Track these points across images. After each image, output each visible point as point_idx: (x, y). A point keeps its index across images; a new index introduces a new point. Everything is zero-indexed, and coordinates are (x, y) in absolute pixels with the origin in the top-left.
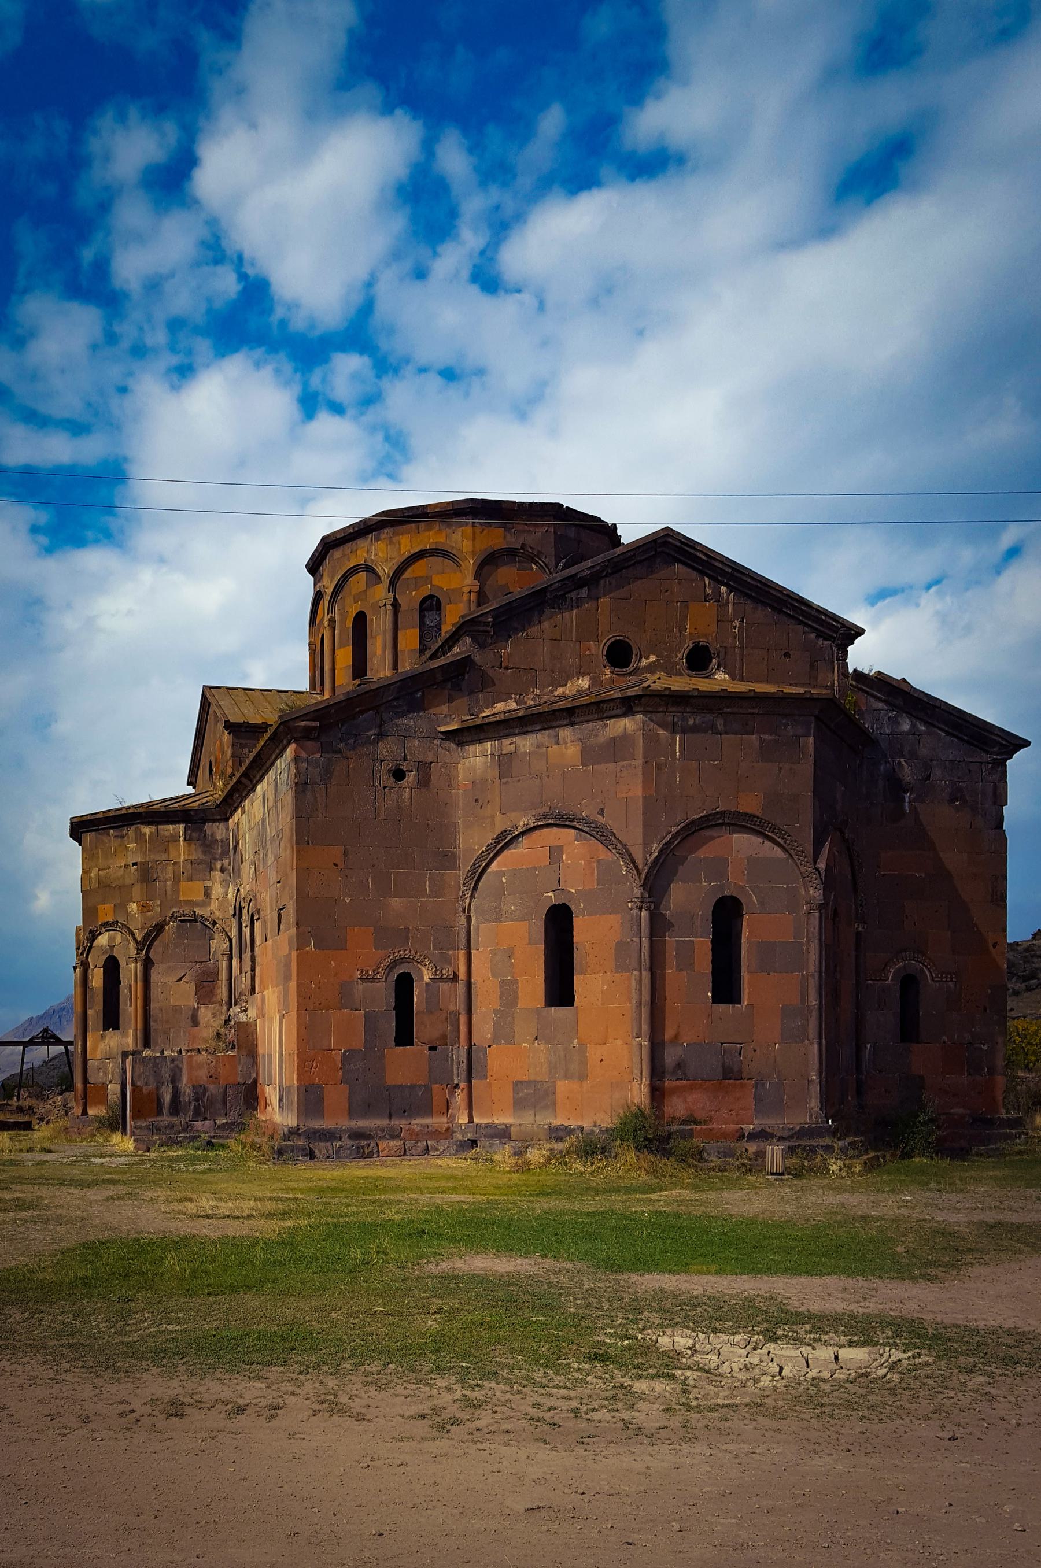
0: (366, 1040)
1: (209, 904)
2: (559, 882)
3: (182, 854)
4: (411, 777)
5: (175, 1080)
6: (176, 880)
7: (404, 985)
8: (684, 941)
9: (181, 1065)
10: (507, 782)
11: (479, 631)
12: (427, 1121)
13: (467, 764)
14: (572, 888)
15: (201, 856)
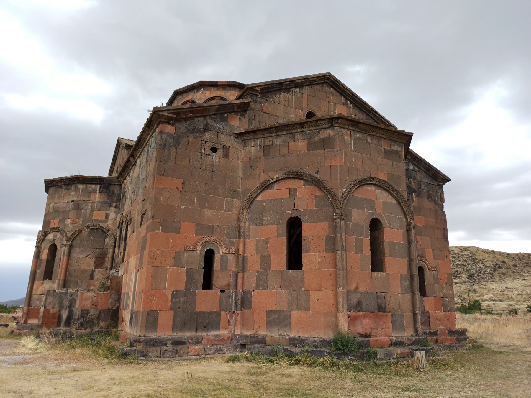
0: (186, 285)
1: (107, 222)
2: (294, 206)
3: (97, 198)
4: (220, 152)
5: (71, 306)
6: (92, 210)
7: (209, 255)
8: (358, 238)
9: (76, 298)
10: (268, 158)
11: (253, 94)
12: (217, 333)
13: (247, 150)
14: (302, 208)
15: (106, 200)
